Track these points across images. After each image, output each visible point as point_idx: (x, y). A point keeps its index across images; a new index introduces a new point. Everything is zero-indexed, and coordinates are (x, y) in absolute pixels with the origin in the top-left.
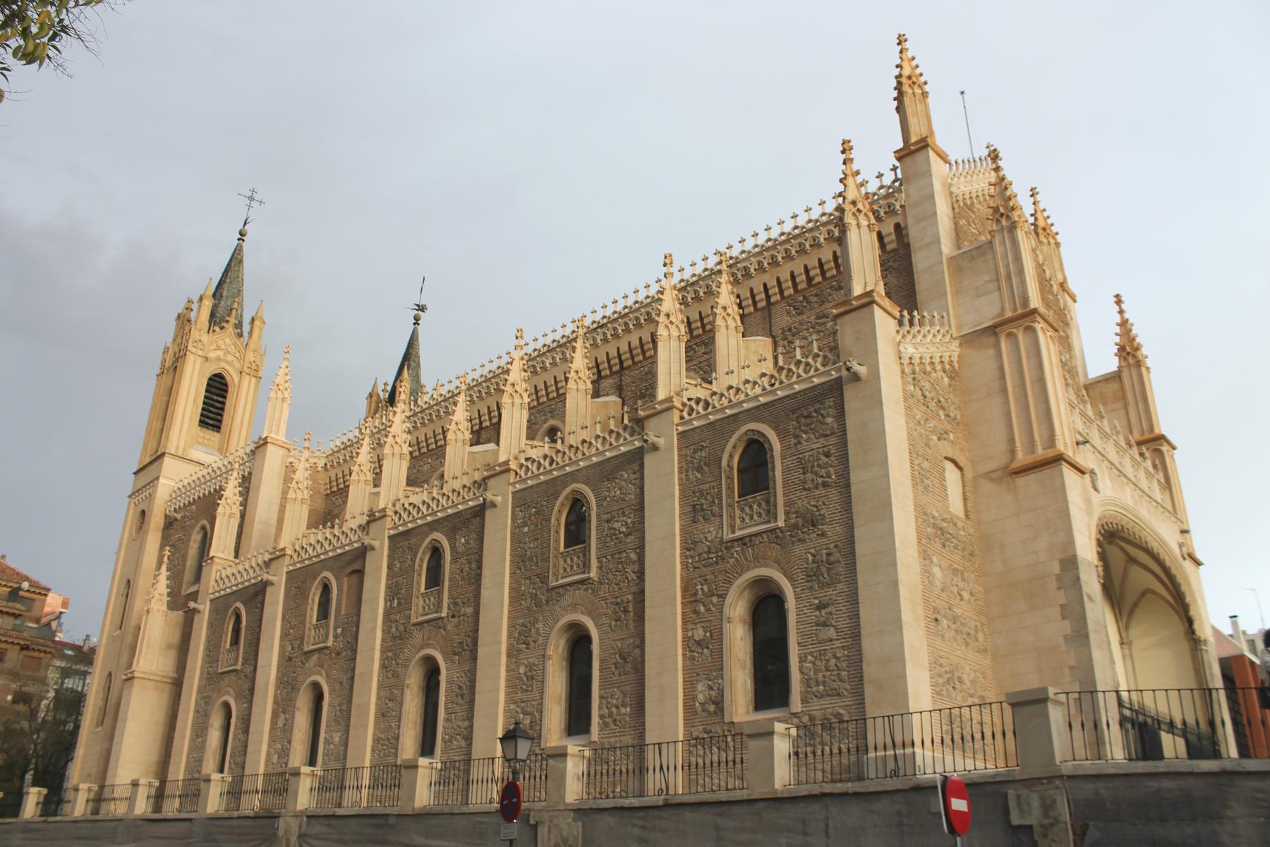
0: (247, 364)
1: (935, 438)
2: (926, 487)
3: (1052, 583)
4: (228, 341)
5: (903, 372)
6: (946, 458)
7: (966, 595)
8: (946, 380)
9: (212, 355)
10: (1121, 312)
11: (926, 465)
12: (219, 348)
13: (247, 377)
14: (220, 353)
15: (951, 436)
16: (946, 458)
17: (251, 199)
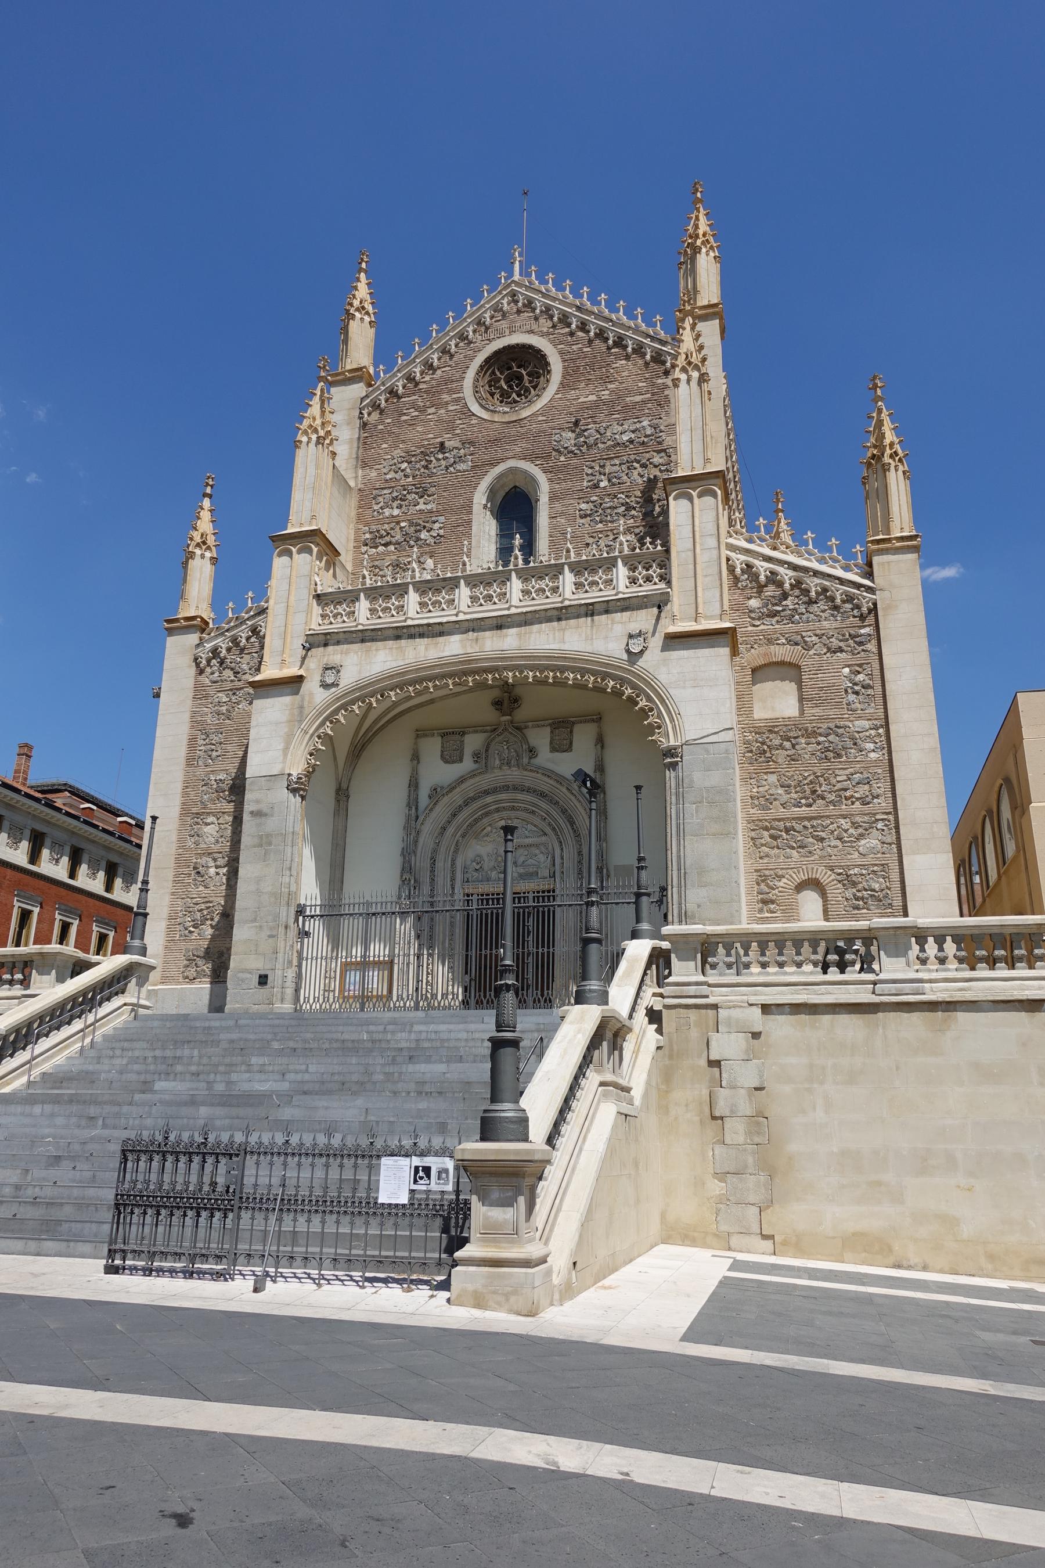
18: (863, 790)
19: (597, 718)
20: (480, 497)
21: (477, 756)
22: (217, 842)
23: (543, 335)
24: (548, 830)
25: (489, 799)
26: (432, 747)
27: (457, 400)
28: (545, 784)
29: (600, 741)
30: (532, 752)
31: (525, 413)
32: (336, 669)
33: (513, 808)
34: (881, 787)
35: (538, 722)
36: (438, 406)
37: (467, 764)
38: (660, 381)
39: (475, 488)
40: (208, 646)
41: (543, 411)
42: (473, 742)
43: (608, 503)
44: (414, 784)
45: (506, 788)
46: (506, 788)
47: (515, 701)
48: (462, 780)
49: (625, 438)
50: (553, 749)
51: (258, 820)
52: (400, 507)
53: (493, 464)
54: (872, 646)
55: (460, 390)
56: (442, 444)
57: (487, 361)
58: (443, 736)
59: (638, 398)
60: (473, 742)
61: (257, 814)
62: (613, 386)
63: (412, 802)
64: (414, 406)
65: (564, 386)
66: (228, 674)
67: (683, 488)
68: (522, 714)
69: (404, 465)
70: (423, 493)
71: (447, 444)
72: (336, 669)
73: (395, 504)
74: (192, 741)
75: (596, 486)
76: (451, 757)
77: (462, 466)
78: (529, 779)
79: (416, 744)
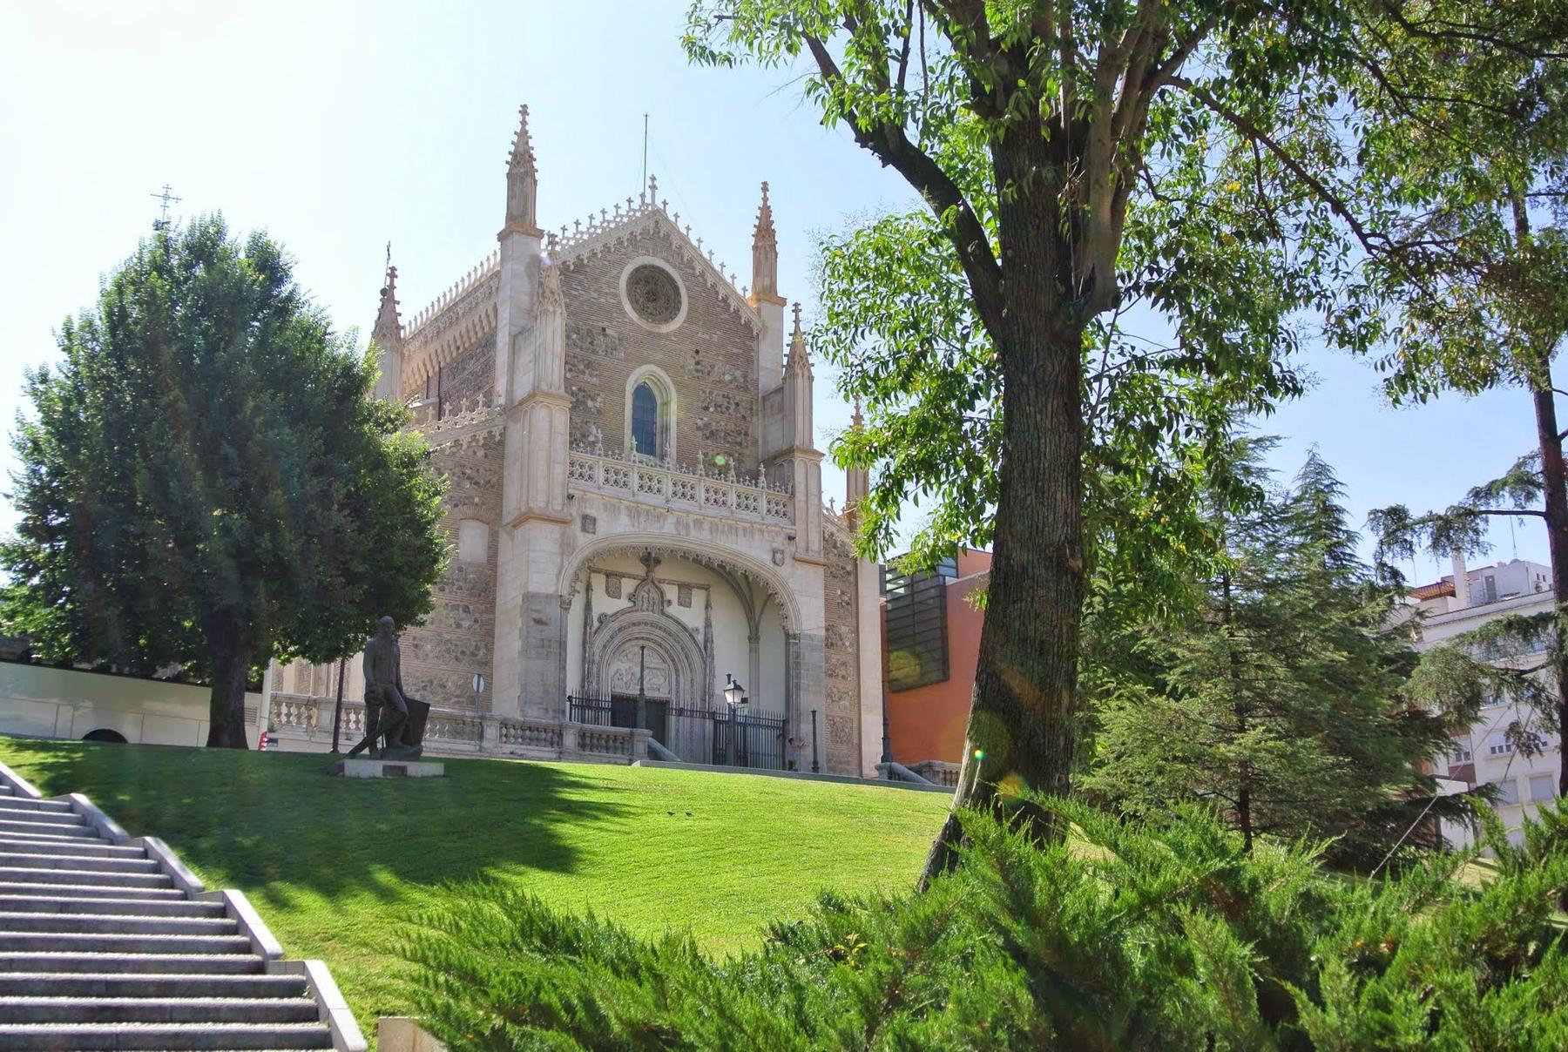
3: (518, 611)
7: (466, 624)
10: (797, 321)
17: (166, 197)
18: (841, 671)
19: (706, 588)
21: (632, 597)
25: (636, 629)
26: (599, 582)
27: (616, 296)
28: (674, 628)
29: (708, 606)
30: (669, 602)
34: (852, 670)
35: (671, 583)
37: (623, 603)
42: (628, 586)
43: (714, 426)
47: (658, 561)
48: (623, 612)
49: (728, 378)
50: (680, 604)
51: (540, 627)
53: (643, 361)
54: (851, 578)
57: (637, 270)
58: (608, 576)
60: (628, 586)
61: (539, 622)
65: (689, 319)
68: (660, 573)
70: (588, 366)
75: (707, 408)
76: (613, 592)
78: (663, 621)
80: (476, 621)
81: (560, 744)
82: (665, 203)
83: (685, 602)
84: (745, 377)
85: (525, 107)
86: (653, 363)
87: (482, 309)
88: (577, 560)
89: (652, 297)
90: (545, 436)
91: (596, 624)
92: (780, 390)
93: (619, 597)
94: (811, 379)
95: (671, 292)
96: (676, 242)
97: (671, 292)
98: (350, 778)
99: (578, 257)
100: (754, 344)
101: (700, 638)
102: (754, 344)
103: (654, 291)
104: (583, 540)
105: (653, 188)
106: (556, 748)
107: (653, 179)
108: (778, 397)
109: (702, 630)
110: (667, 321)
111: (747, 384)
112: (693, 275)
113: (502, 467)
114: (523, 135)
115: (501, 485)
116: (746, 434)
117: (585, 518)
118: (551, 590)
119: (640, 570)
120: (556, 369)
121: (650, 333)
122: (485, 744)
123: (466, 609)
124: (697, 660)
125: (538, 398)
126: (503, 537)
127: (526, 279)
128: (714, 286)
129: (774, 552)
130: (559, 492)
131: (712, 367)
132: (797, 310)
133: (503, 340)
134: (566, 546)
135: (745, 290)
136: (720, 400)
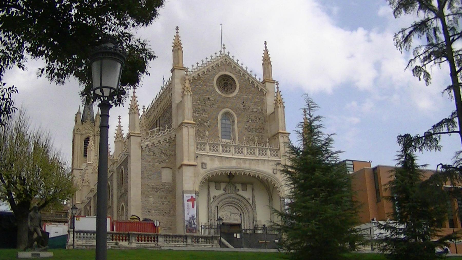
0: (96, 132)
1: (157, 164)
2: (150, 179)
4: (88, 126)
5: (142, 151)
6: (162, 168)
7: (165, 203)
8: (168, 144)
9: (84, 132)
10: (278, 88)
11: (152, 173)
12: (86, 129)
13: (97, 137)
14: (86, 131)
15: (167, 160)
16: (162, 168)
19: (252, 184)
20: (220, 117)
22: (154, 203)
23: (233, 74)
24: (240, 210)
27: (213, 86)
29: (253, 190)
30: (238, 190)
31: (231, 96)
32: (206, 164)
33: (232, 203)
35: (239, 183)
36: (206, 86)
37: (222, 192)
38: (262, 97)
39: (219, 113)
40: (147, 143)
41: (236, 97)
44: (209, 194)
45: (230, 197)
46: (230, 197)
48: (222, 195)
49: (255, 110)
50: (243, 190)
52: (198, 113)
55: (213, 83)
56: (209, 98)
57: (220, 77)
58: (215, 182)
59: (258, 100)
60: (223, 186)
62: (251, 95)
63: (208, 200)
64: (200, 83)
66: (151, 153)
67: (282, 134)
69: (198, 102)
70: (204, 111)
71: (210, 99)
72: (206, 164)
73: (197, 112)
74: (143, 173)
75: (248, 121)
76: (218, 188)
77: (213, 106)
79: (209, 184)
80: (169, 202)
81: (186, 242)
82: (229, 53)
83: (244, 190)
84: (262, 109)
85: (177, 27)
86: (228, 108)
87: (168, 96)
88: (200, 178)
89: (226, 85)
90: (187, 137)
91: (212, 200)
92: (274, 112)
93: (220, 189)
94: (284, 107)
95: (233, 83)
96: (233, 65)
97: (233, 83)
98: (21, 259)
99: (198, 74)
100: (264, 98)
101: (251, 202)
102: (264, 98)
103: (226, 83)
104: (202, 171)
105: (224, 48)
106: (185, 243)
107: (224, 45)
108: (273, 115)
109: (251, 199)
110: (231, 93)
111: (262, 112)
112: (241, 76)
113: (175, 149)
114: (177, 37)
115: (175, 155)
116: (263, 129)
117: (203, 163)
118: (192, 189)
119: (227, 179)
120: (190, 114)
121: (225, 97)
122: (159, 243)
123: (166, 198)
124: (250, 209)
125: (183, 124)
126: (177, 172)
127: (180, 84)
128: (248, 78)
129: (273, 169)
130: (193, 156)
131: (249, 107)
132: (277, 84)
133: (174, 106)
134: (196, 175)
135: (260, 79)
136: (253, 118)
